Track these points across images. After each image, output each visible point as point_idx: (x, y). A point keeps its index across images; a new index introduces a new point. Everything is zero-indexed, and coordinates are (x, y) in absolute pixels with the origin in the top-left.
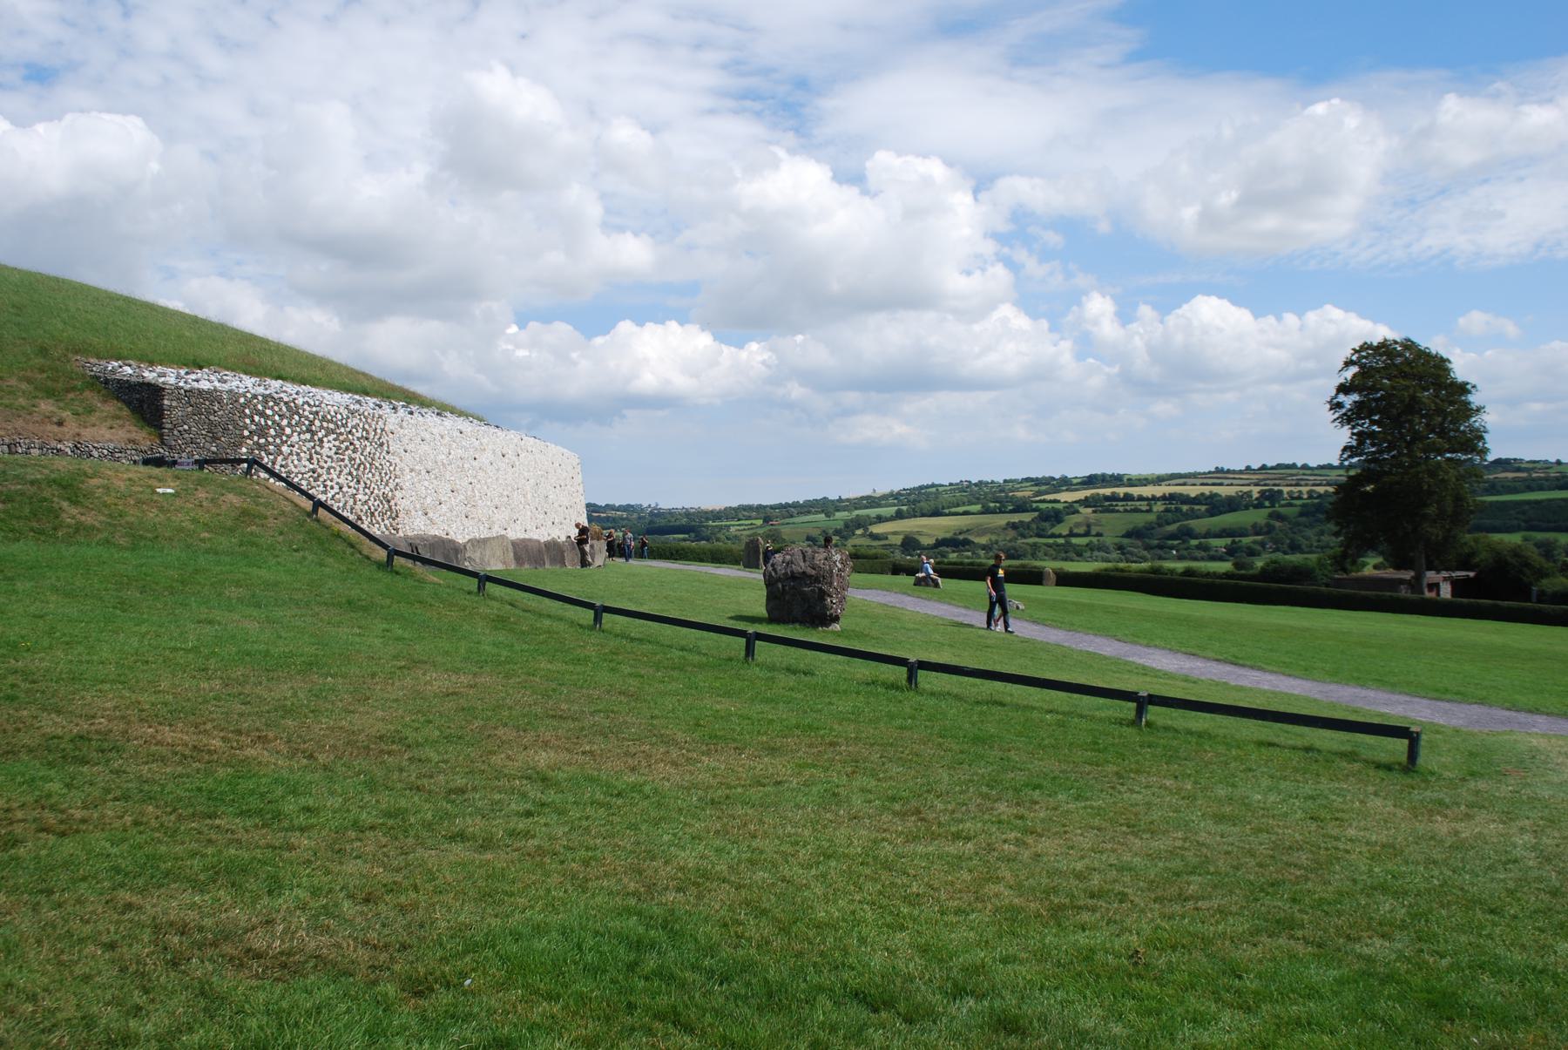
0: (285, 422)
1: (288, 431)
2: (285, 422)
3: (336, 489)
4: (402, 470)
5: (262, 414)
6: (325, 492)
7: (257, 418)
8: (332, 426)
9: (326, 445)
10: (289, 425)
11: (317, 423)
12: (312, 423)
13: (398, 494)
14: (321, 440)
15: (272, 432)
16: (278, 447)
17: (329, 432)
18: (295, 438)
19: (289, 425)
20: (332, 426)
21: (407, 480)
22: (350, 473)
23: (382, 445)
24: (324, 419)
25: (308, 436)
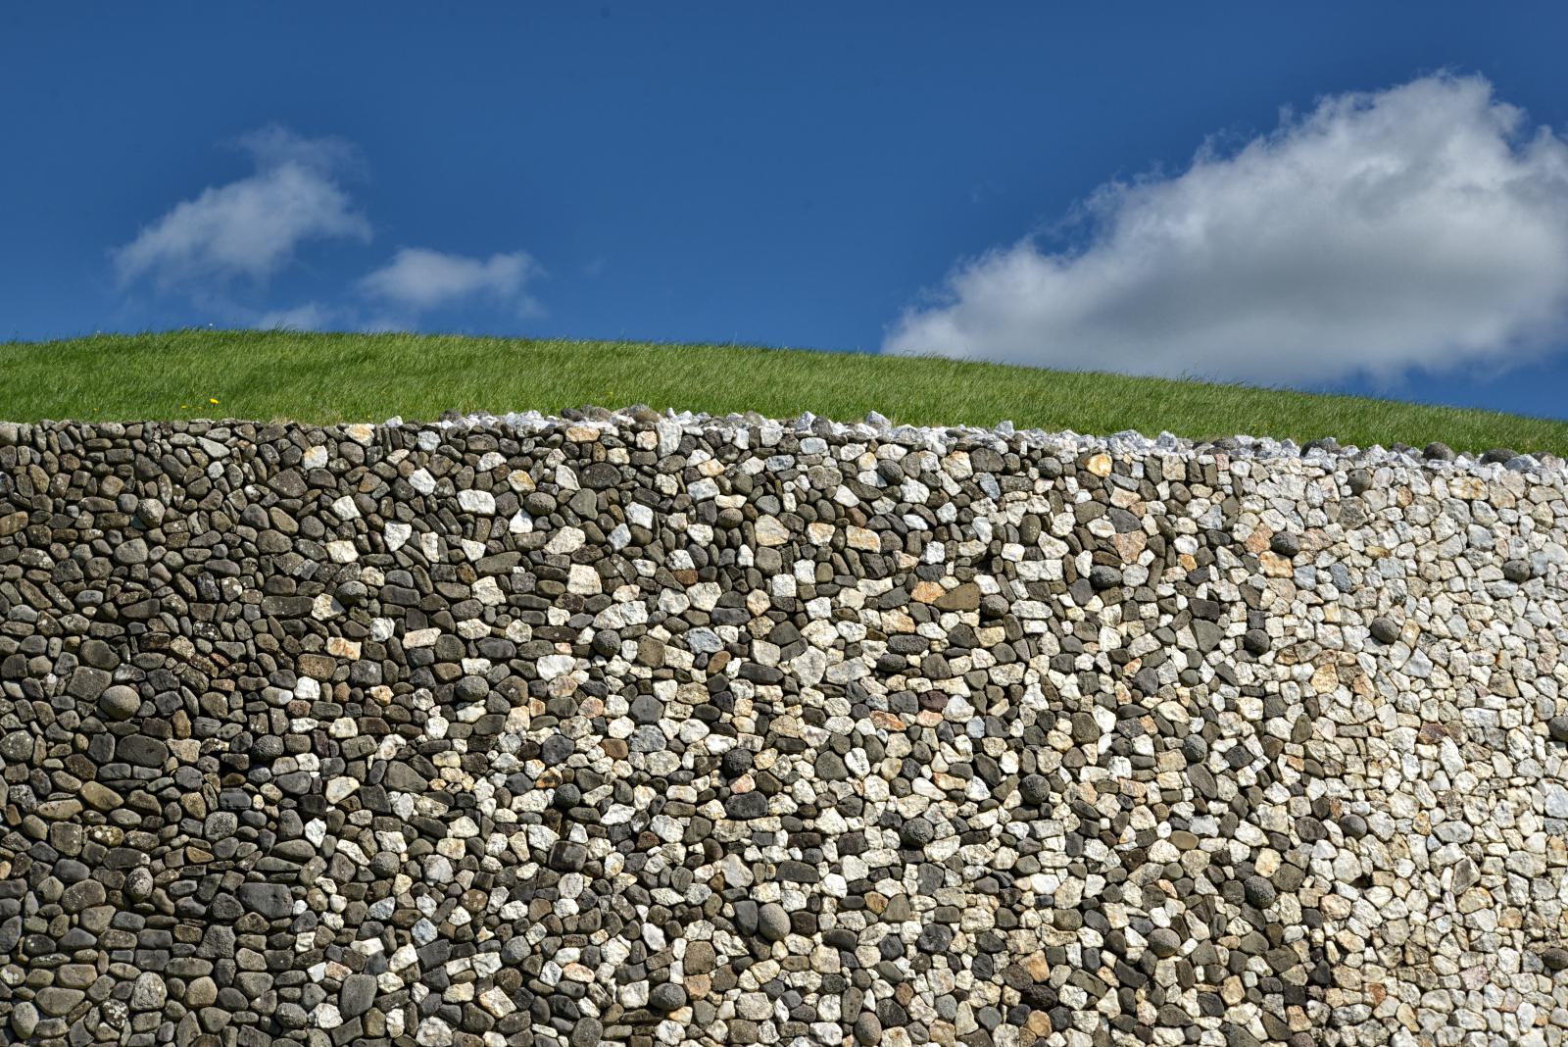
0: (571, 538)
1: (583, 579)
2: (571, 538)
3: (882, 849)
4: (1362, 734)
5: (435, 513)
6: (802, 873)
7: (397, 535)
8: (863, 538)
9: (823, 633)
10: (596, 551)
11: (769, 531)
12: (731, 531)
13: (1333, 860)
14: (792, 614)
15: (487, 591)
16: (518, 663)
17: (840, 567)
18: (628, 609)
19: (596, 551)
20: (863, 538)
21: (1398, 787)
22: (980, 765)
23: (1216, 607)
24: (815, 504)
25: (707, 597)
